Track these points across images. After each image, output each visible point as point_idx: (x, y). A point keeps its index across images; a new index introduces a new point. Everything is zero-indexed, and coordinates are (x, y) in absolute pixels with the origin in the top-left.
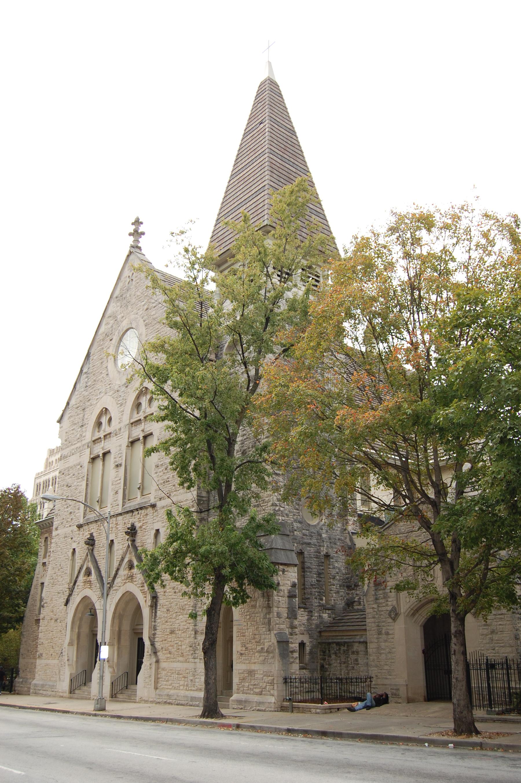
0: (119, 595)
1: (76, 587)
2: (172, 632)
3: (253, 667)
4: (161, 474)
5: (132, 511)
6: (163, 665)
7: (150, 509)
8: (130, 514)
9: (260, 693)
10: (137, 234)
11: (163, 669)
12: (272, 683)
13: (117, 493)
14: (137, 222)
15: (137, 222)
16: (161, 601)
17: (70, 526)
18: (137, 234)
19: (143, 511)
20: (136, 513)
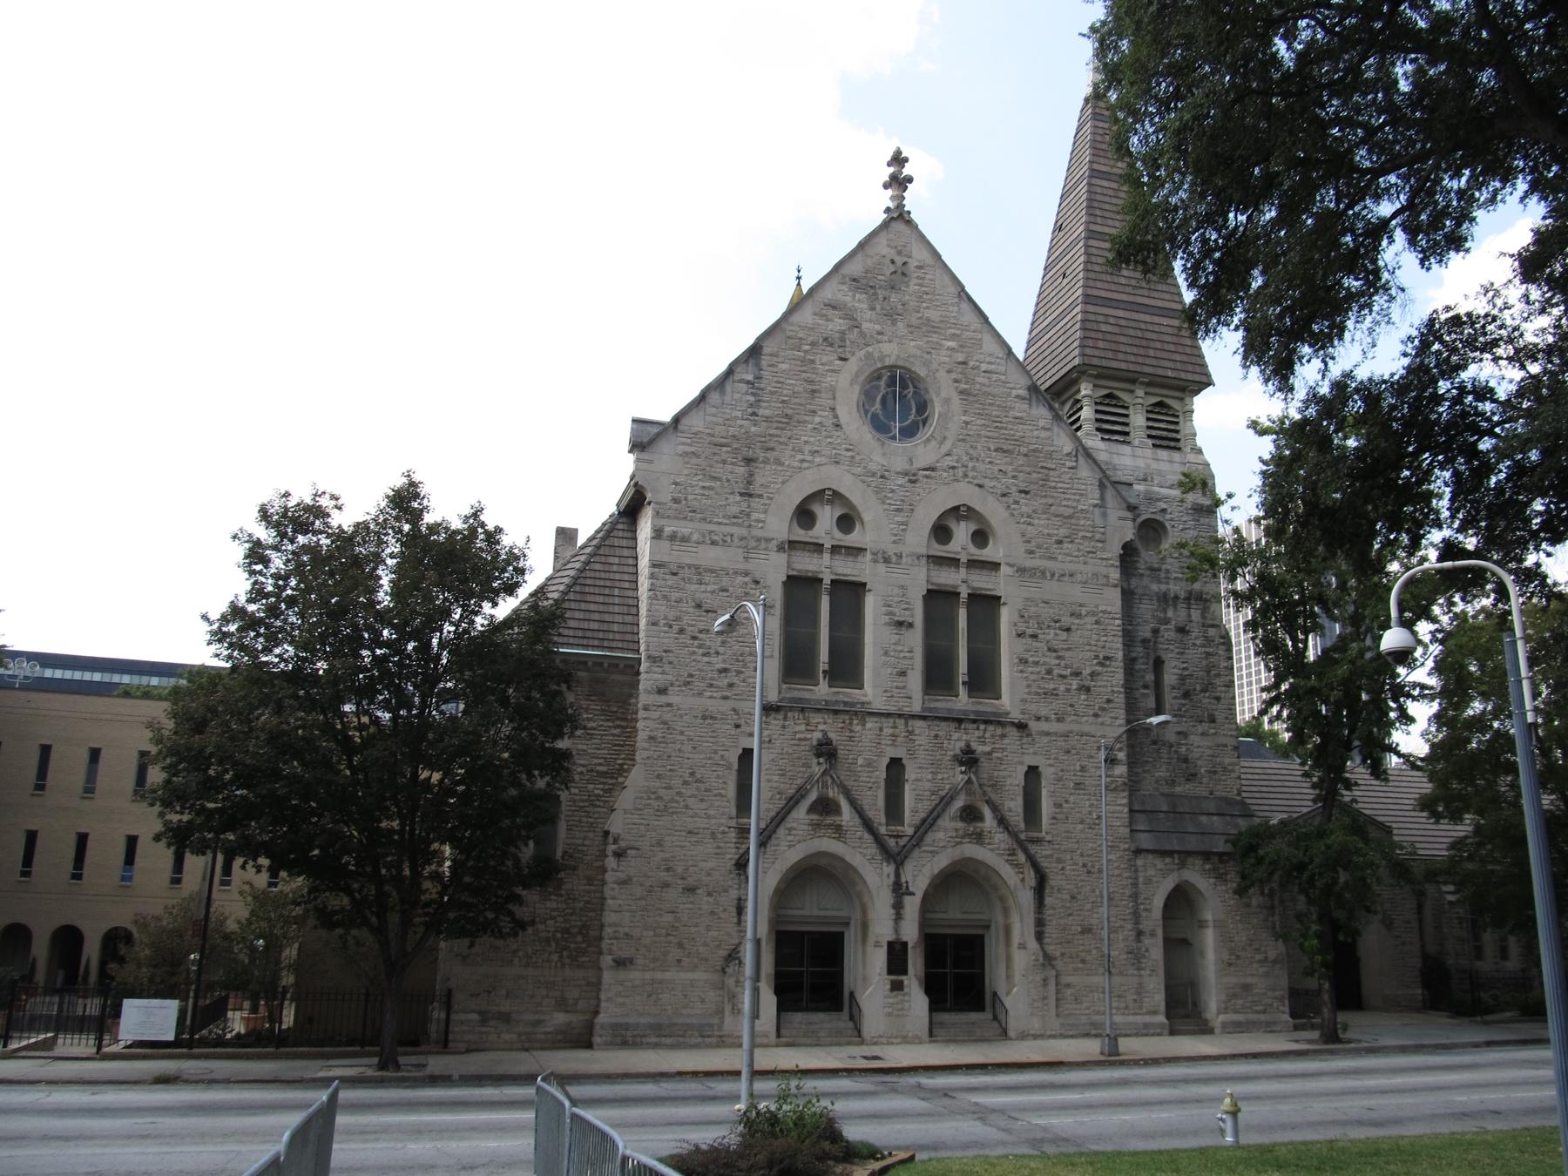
0: (942, 862)
1: (781, 831)
2: (1087, 930)
3: (1249, 980)
4: (1033, 677)
5: (960, 721)
6: (1065, 979)
7: (1013, 732)
8: (953, 725)
9: (1264, 1012)
10: (899, 182)
11: (1068, 986)
12: (1281, 999)
13: (903, 673)
14: (898, 160)
15: (898, 160)
16: (1054, 880)
17: (726, 698)
18: (899, 182)
19: (991, 728)
20: (971, 726)
